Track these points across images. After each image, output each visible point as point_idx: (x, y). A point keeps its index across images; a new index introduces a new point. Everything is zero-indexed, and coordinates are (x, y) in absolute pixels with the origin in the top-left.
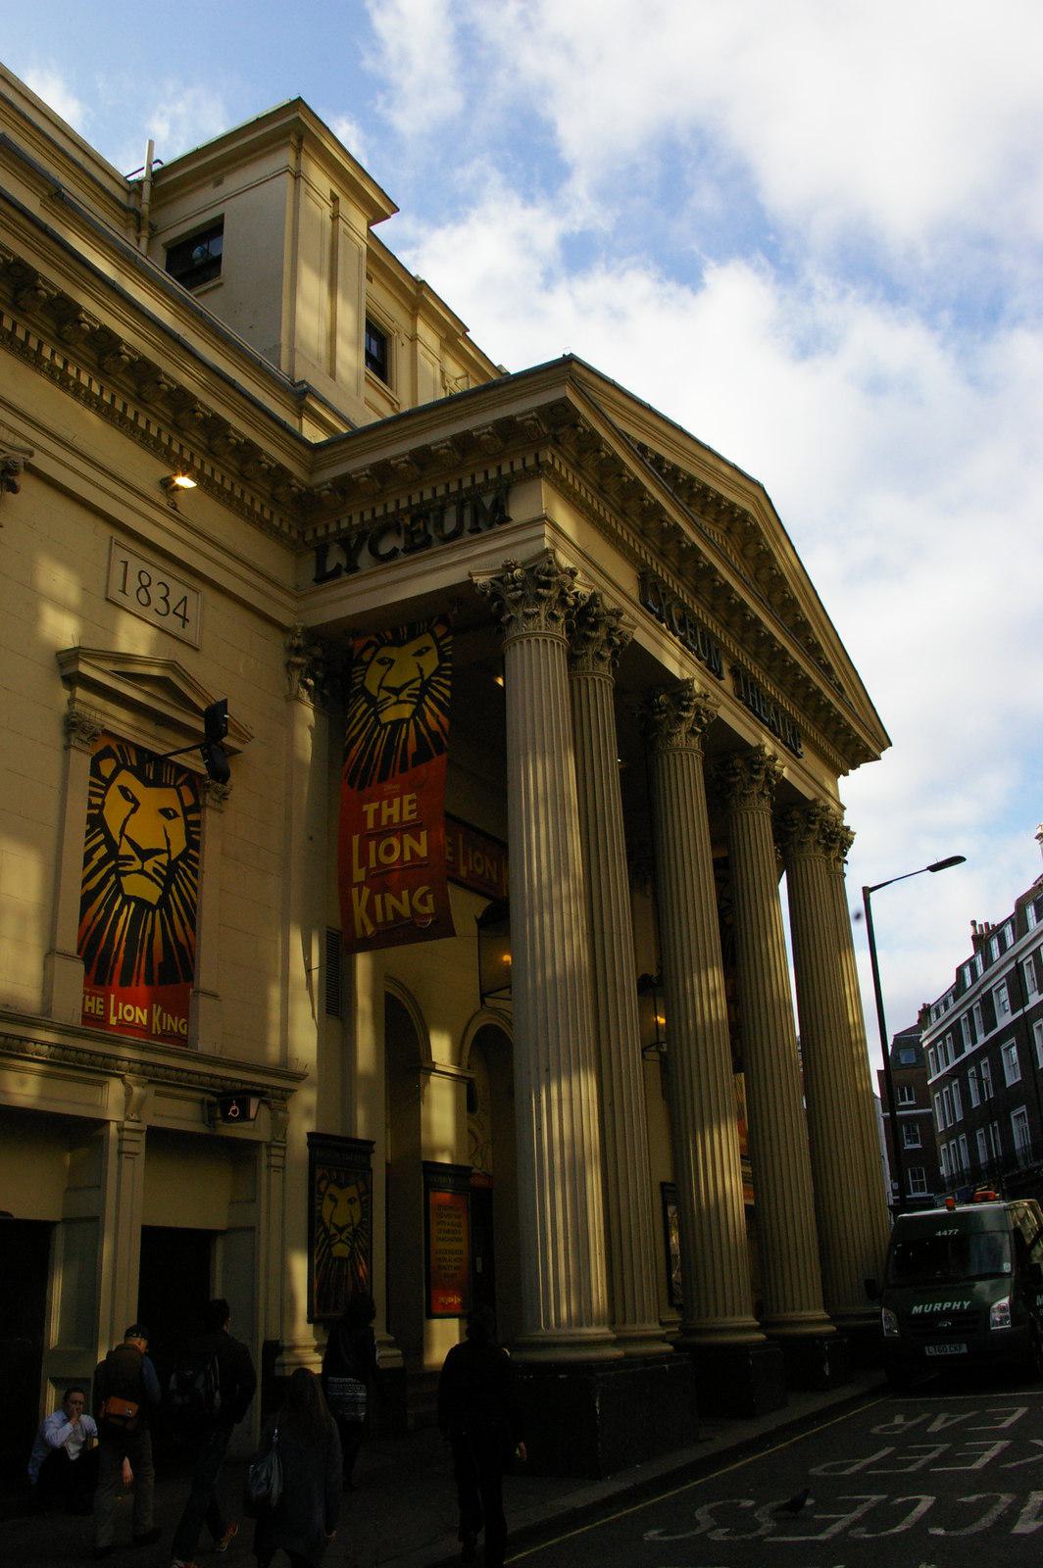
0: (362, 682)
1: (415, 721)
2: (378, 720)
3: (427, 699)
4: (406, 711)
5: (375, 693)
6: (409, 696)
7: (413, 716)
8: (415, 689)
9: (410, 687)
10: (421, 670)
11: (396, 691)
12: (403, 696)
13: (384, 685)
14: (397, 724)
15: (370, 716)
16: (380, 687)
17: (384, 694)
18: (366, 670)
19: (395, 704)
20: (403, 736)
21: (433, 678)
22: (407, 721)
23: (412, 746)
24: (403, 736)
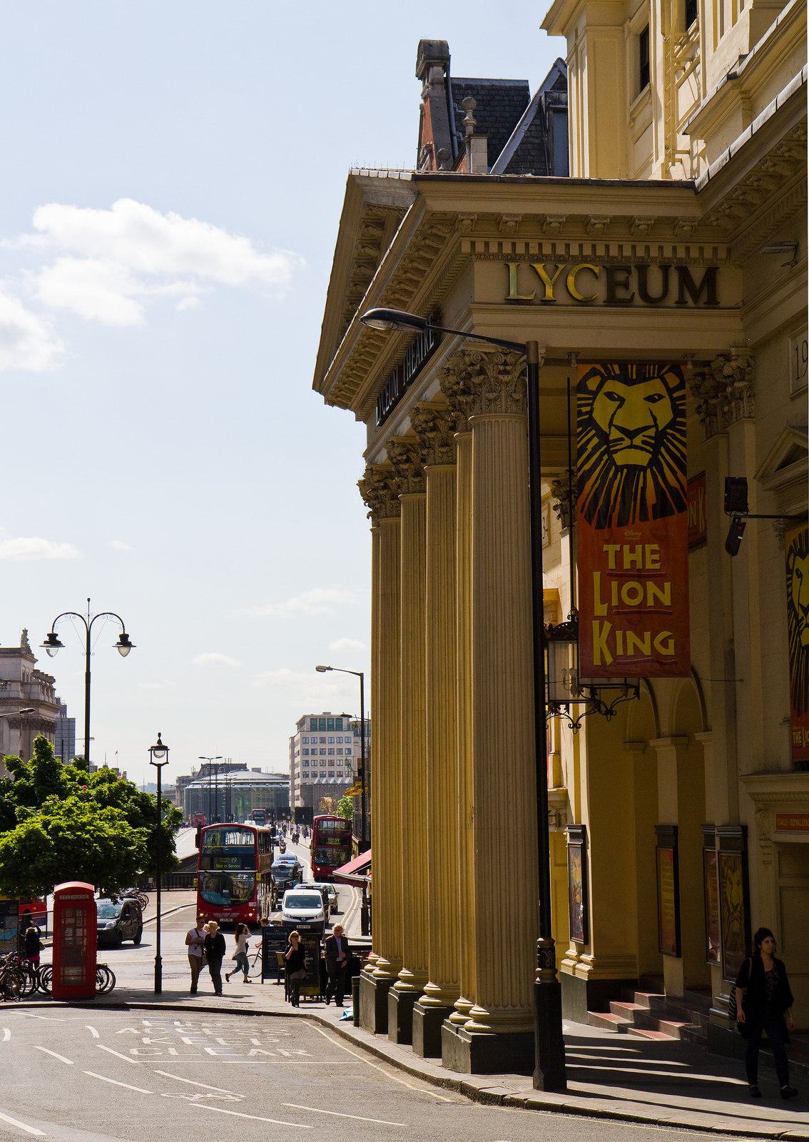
0: (590, 413)
1: (652, 471)
3: (663, 450)
4: (642, 458)
6: (643, 442)
8: (649, 437)
9: (645, 433)
10: (655, 419)
11: (631, 434)
12: (638, 441)
14: (633, 470)
16: (611, 424)
18: (594, 399)
20: (641, 484)
21: (668, 431)
22: (644, 469)
24: (641, 484)
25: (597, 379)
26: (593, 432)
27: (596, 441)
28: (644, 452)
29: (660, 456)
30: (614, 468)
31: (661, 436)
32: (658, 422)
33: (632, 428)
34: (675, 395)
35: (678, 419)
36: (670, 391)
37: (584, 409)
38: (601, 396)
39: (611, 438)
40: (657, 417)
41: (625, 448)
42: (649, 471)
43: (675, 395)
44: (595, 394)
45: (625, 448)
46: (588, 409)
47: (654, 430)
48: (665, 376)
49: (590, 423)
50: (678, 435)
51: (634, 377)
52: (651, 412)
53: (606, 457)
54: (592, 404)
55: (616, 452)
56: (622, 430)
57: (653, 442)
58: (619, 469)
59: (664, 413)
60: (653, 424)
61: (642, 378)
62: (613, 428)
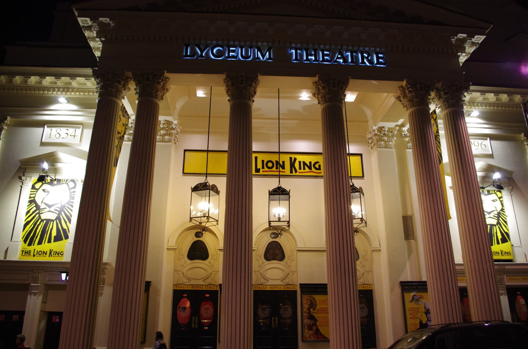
0: (34, 197)
2: (40, 217)
3: (63, 213)
4: (53, 216)
6: (55, 210)
7: (56, 219)
11: (50, 206)
12: (52, 209)
13: (43, 202)
14: (48, 221)
16: (42, 202)
17: (45, 206)
18: (37, 192)
19: (48, 211)
20: (51, 227)
22: (53, 221)
23: (54, 233)
24: (51, 227)
26: (34, 205)
27: (35, 209)
28: (54, 213)
33: (50, 204)
37: (32, 196)
38: (40, 190)
39: (41, 208)
44: (38, 190)
46: (34, 196)
53: (38, 215)
54: (35, 194)
55: (42, 213)
58: (42, 220)
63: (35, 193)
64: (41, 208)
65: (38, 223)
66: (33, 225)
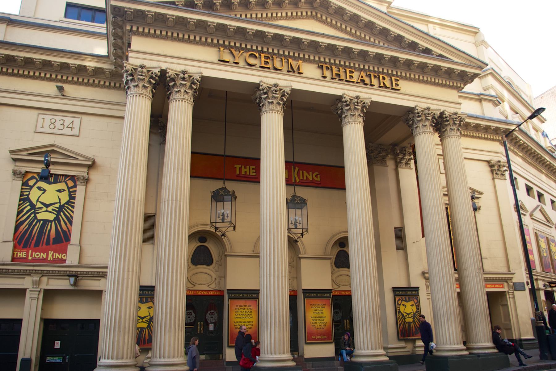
0: (28, 195)
1: (55, 224)
2: (35, 217)
3: (62, 213)
4: (51, 217)
5: (35, 203)
6: (53, 210)
7: (55, 219)
11: (47, 206)
14: (46, 221)
15: (31, 214)
16: (38, 201)
17: (40, 205)
18: (31, 189)
19: (45, 211)
20: (49, 228)
22: (51, 221)
24: (49, 228)
25: (34, 181)
26: (28, 204)
27: (29, 207)
28: (52, 214)
29: (60, 216)
30: (36, 220)
31: (61, 208)
32: (61, 201)
34: (71, 190)
35: (71, 201)
36: (69, 188)
37: (25, 193)
38: (35, 188)
39: (37, 207)
40: (61, 199)
41: (43, 212)
42: (53, 223)
43: (71, 190)
44: (32, 187)
45: (43, 212)
46: (27, 193)
47: (59, 204)
48: (67, 182)
49: (28, 199)
50: (70, 207)
51: (52, 181)
52: (58, 197)
53: (33, 215)
54: (29, 192)
55: (38, 213)
56: (42, 203)
57: (57, 210)
58: (39, 221)
59: (65, 197)
60: (58, 202)
61: (56, 182)
62: (38, 202)
63: (29, 190)
64: (37, 207)
65: (34, 224)
66: (27, 226)
